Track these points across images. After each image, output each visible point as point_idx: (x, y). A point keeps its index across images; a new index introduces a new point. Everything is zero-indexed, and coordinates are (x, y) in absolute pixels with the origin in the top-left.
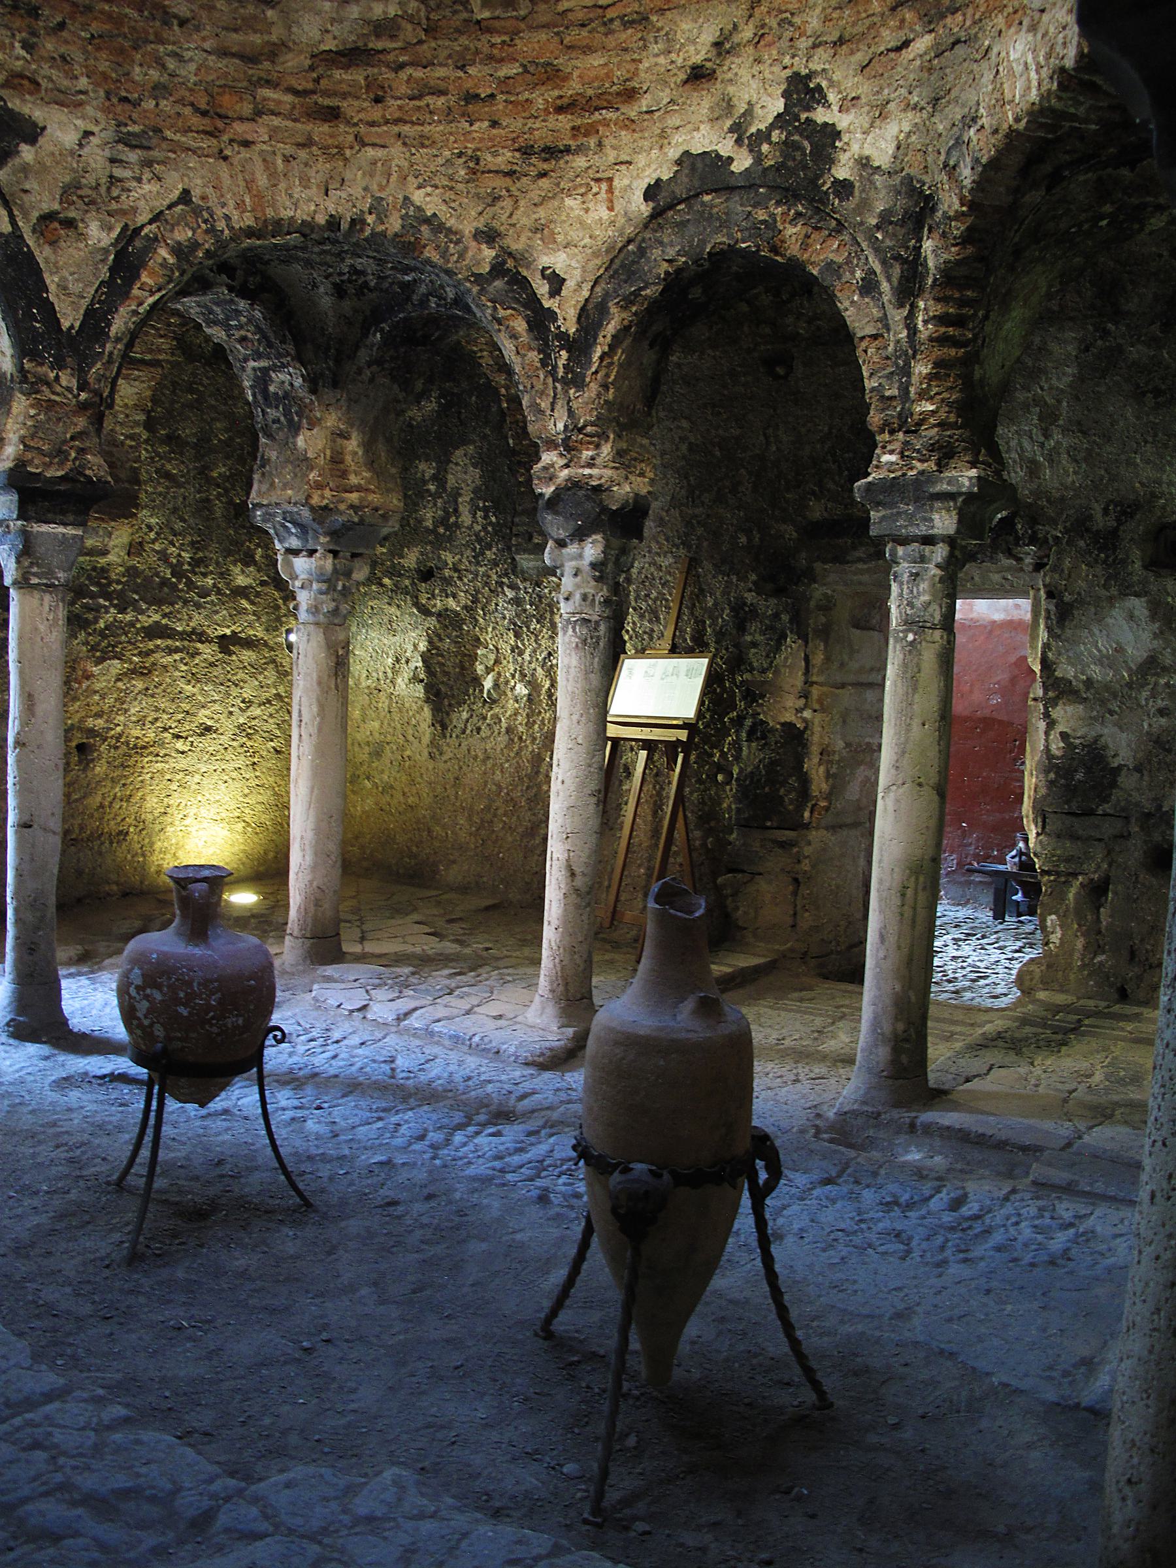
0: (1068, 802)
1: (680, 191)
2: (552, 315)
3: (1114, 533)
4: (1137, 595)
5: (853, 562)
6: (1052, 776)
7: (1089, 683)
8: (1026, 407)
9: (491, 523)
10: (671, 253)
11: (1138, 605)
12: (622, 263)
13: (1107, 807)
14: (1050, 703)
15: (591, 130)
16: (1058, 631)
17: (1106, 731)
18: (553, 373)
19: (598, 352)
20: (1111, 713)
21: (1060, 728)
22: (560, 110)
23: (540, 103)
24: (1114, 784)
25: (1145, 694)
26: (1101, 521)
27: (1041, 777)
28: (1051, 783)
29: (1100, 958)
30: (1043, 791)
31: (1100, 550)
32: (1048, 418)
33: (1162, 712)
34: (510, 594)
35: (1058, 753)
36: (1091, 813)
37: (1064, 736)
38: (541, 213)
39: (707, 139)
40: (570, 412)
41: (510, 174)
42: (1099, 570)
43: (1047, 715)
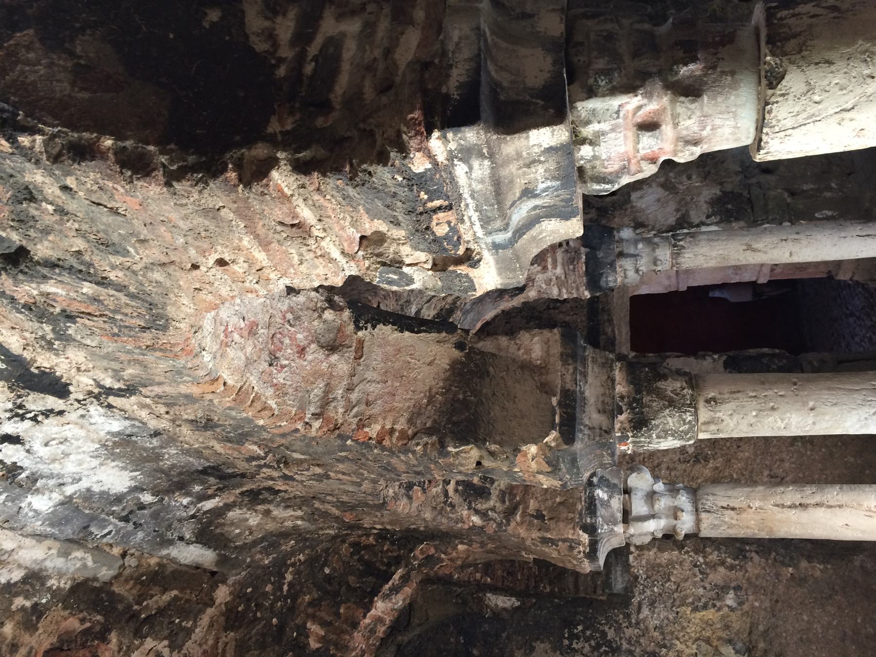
0: (746, 210)
3: (598, 209)
4: (630, 196)
5: (614, 334)
6: (732, 219)
7: (677, 210)
9: (583, 631)
13: (745, 193)
16: (650, 227)
17: (703, 200)
20: (692, 199)
21: (704, 219)
24: (732, 193)
25: (681, 187)
27: (734, 224)
28: (737, 219)
29: (833, 185)
30: (742, 223)
31: (607, 213)
33: (689, 178)
34: (645, 612)
35: (718, 218)
36: (749, 200)
37: (708, 217)
42: (617, 213)
43: (698, 226)
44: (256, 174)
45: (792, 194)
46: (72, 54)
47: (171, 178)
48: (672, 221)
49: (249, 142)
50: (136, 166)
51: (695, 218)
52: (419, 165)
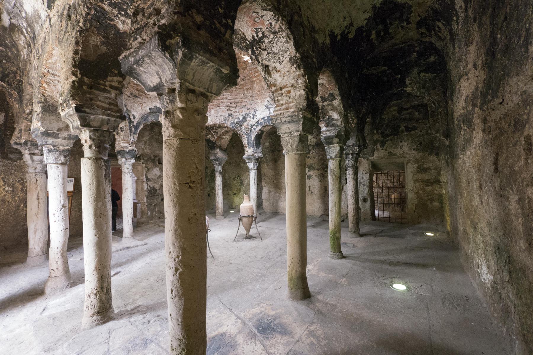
1: (154, 110)
2: (133, 122)
8: (142, 141)
10: (153, 119)
11: (158, 168)
12: (144, 118)
14: (147, 182)
15: (141, 95)
18: (131, 131)
19: (139, 130)
22: (137, 90)
23: (135, 88)
26: (153, 158)
32: (145, 143)
38: (132, 104)
39: (159, 105)
40: (134, 138)
41: (129, 97)
44: (74, 74)
45: (155, 205)
46: (101, 45)
47: (74, 59)
48: (149, 177)
49: (81, 73)
50: (76, 52)
51: (149, 183)
52: (70, 102)
